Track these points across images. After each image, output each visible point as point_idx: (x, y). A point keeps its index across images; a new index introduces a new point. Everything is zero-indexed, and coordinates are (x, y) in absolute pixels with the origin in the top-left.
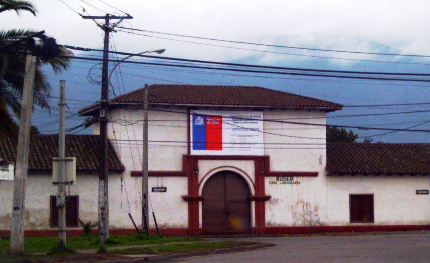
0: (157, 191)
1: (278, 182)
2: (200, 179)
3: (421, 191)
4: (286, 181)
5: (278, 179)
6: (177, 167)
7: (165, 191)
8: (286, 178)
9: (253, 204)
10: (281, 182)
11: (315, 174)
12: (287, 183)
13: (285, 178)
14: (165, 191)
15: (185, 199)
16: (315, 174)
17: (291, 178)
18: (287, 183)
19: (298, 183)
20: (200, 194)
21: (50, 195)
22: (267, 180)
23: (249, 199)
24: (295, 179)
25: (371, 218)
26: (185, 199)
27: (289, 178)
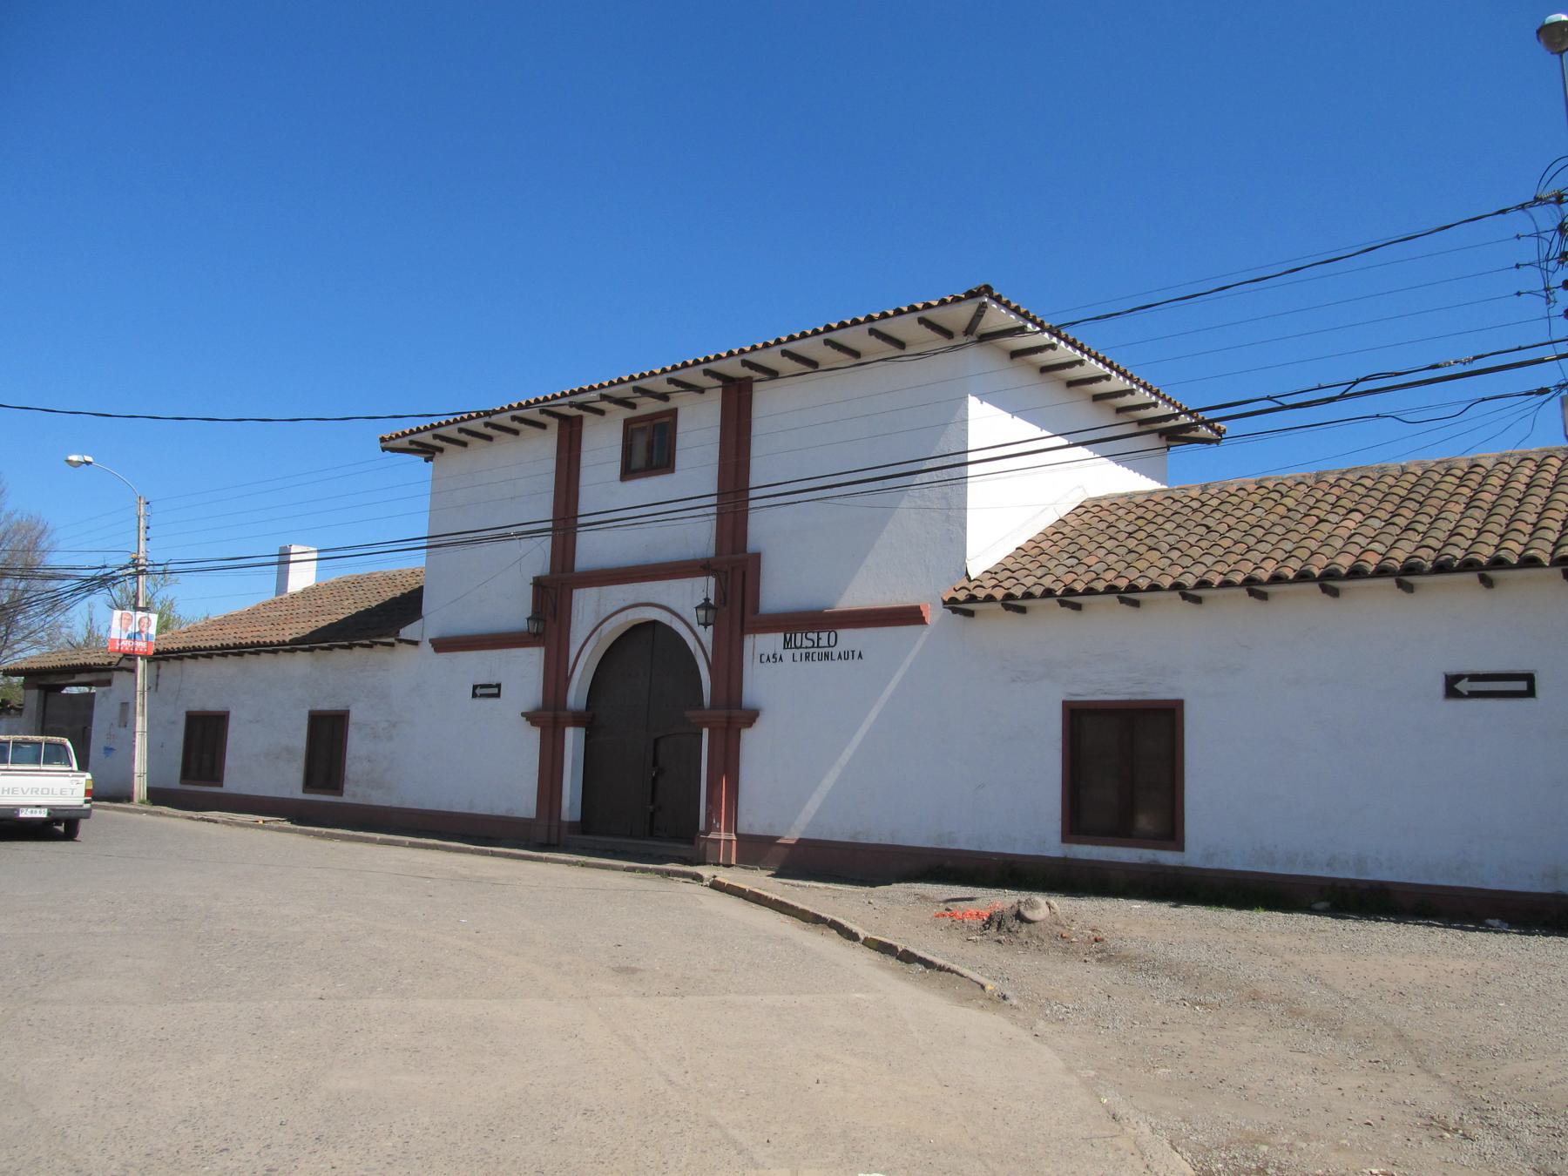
0: (482, 696)
1: (787, 654)
6: (516, 611)
7: (498, 695)
8: (813, 636)
10: (798, 652)
11: (910, 616)
13: (810, 635)
14: (1530, 693)
15: (532, 717)
17: (833, 635)
19: (856, 654)
21: (309, 708)
23: (587, 720)
24: (848, 638)
27: (824, 636)
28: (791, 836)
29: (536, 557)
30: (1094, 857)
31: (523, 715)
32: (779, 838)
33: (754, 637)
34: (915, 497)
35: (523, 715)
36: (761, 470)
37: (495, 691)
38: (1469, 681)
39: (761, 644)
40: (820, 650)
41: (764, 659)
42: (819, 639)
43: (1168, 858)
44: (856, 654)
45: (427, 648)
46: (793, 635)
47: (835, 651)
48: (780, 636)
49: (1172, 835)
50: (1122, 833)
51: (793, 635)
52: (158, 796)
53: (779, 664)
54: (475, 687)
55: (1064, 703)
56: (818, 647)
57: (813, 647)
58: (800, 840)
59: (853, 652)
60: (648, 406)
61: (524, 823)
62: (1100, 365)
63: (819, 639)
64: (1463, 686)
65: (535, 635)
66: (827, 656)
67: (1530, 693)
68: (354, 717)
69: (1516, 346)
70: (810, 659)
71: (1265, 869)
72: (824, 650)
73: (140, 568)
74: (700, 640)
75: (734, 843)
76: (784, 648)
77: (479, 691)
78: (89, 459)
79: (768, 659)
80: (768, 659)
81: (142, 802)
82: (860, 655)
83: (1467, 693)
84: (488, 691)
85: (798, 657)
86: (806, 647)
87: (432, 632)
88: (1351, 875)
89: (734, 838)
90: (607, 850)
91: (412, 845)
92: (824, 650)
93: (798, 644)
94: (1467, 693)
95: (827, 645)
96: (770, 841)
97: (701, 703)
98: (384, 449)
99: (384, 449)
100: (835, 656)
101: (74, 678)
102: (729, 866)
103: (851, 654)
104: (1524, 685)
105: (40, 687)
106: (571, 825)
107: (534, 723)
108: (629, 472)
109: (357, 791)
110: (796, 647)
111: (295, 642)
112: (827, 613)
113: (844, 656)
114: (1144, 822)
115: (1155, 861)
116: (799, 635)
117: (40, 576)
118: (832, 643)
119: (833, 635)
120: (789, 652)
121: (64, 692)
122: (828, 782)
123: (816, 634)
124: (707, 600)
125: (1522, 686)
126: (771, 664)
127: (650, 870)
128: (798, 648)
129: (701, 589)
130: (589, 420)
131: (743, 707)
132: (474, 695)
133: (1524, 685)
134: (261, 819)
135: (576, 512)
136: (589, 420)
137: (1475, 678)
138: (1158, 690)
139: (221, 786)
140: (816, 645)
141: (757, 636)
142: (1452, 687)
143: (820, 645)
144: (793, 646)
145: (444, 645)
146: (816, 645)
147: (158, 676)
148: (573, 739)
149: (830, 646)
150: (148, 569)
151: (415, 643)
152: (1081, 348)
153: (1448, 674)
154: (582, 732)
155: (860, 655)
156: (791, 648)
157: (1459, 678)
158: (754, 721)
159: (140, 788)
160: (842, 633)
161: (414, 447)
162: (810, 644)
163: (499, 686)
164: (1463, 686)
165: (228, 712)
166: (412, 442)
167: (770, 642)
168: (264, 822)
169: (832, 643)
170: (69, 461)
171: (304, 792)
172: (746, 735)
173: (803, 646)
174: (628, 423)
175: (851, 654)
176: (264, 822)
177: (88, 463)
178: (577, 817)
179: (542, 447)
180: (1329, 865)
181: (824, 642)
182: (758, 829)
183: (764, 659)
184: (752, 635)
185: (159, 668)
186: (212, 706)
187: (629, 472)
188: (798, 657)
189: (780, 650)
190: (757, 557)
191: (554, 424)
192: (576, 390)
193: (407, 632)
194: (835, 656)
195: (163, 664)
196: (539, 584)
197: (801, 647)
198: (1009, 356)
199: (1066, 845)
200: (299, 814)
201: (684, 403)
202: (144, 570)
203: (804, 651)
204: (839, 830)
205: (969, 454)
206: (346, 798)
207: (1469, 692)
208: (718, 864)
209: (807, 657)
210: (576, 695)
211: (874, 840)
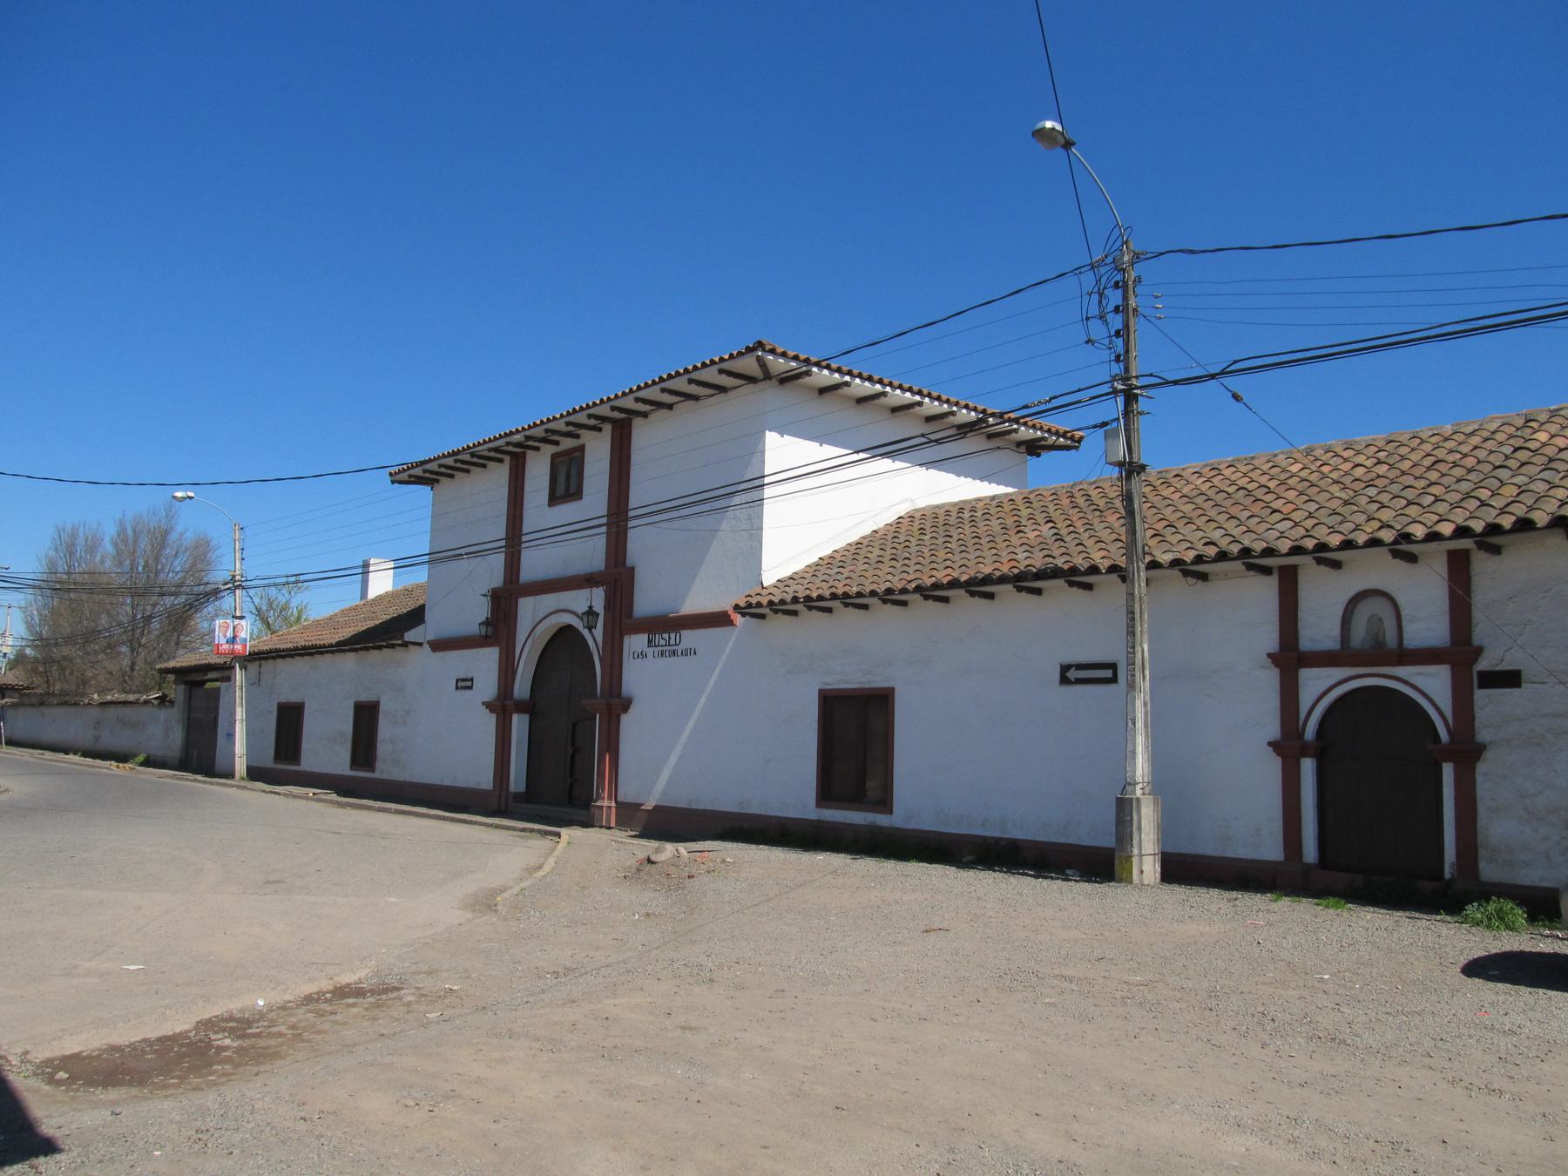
1: (650, 651)
3: (1080, 667)
7: (470, 688)
8: (666, 636)
10: (656, 649)
15: (489, 706)
21: (354, 699)
24: (689, 637)
26: (489, 706)
27: (673, 635)
28: (649, 805)
29: (491, 571)
31: (483, 703)
32: (642, 805)
35: (483, 703)
36: (639, 495)
37: (469, 684)
41: (636, 656)
42: (670, 638)
43: (881, 820)
45: (427, 647)
47: (679, 649)
49: (884, 803)
50: (856, 799)
52: (255, 774)
53: (645, 659)
54: (457, 681)
55: (821, 691)
56: (669, 645)
60: (567, 443)
62: (908, 395)
63: (670, 638)
65: (486, 637)
66: (674, 653)
68: (382, 708)
69: (1077, 389)
71: (943, 829)
73: (236, 584)
74: (595, 638)
75: (613, 810)
77: (460, 684)
78: (191, 494)
81: (243, 779)
82: (695, 653)
84: (465, 684)
86: (662, 646)
87: (430, 637)
88: (996, 834)
89: (613, 804)
96: (636, 807)
97: (596, 694)
98: (393, 482)
99: (393, 482)
100: (680, 653)
101: (206, 675)
102: (609, 828)
105: (185, 683)
106: (517, 796)
107: (491, 711)
108: (554, 499)
109: (386, 769)
110: (655, 646)
111: (339, 644)
112: (673, 617)
113: (686, 653)
116: (657, 636)
120: (651, 649)
121: (206, 687)
122: (673, 759)
124: (591, 607)
126: (639, 660)
127: (514, 829)
129: (596, 598)
130: (530, 453)
131: (623, 695)
132: (457, 688)
134: (310, 791)
136: (530, 453)
138: (880, 682)
139: (299, 764)
141: (632, 636)
145: (439, 645)
147: (260, 673)
148: (519, 723)
149: (676, 645)
150: (244, 584)
151: (420, 644)
152: (880, 382)
154: (526, 718)
158: (629, 708)
159: (240, 767)
160: (685, 633)
161: (412, 479)
163: (472, 680)
165: (304, 703)
166: (410, 476)
168: (314, 794)
170: (174, 497)
171: (351, 769)
172: (625, 719)
174: (554, 457)
176: (314, 794)
177: (191, 498)
178: (522, 788)
179: (498, 476)
181: (672, 642)
185: (260, 666)
186: (293, 698)
187: (554, 499)
188: (656, 653)
190: (633, 569)
191: (507, 458)
192: (508, 432)
193: (410, 636)
194: (680, 653)
195: (263, 662)
197: (658, 645)
198: (817, 393)
199: (820, 810)
200: (346, 788)
201: (587, 437)
202: (240, 585)
204: (682, 798)
205: (766, 478)
206: (377, 775)
207: (1075, 679)
208: (601, 827)
209: (662, 654)
210: (522, 687)
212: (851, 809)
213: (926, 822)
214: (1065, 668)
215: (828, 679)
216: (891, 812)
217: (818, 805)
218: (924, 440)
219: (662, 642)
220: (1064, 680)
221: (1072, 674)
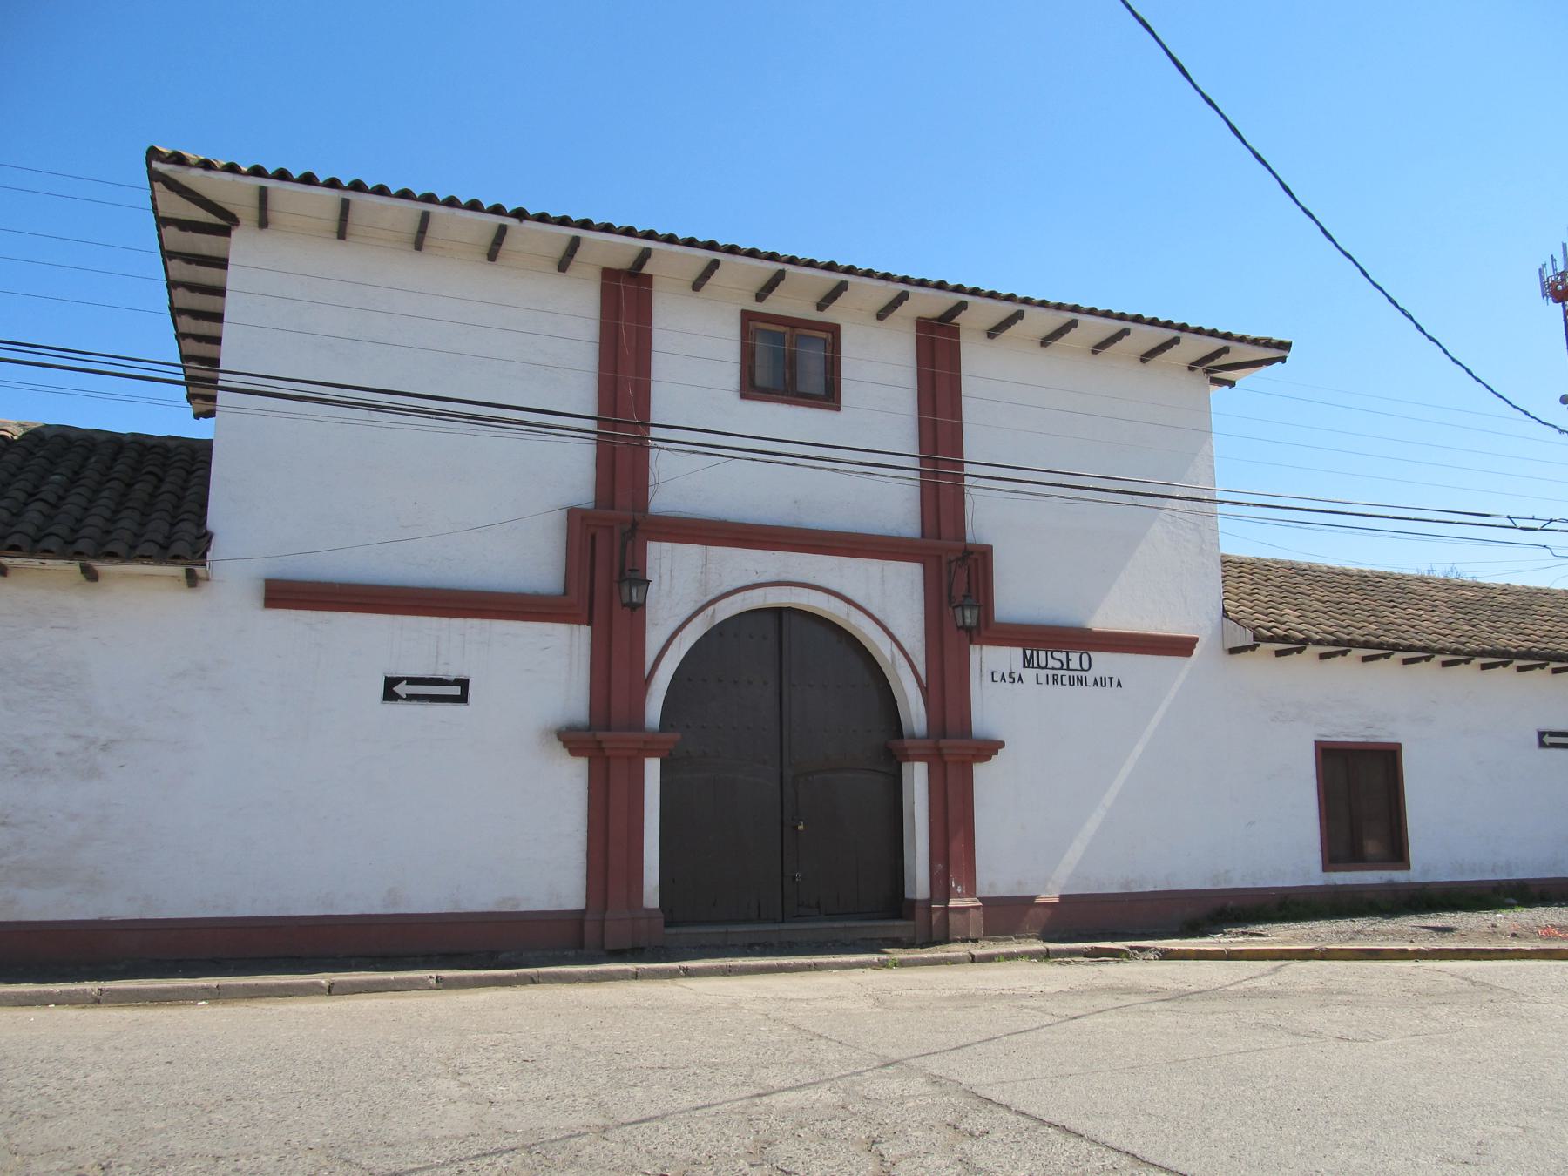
0: (411, 698)
1: (1029, 674)
2: (654, 640)
4: (1060, 673)
5: (1027, 662)
8: (1063, 656)
9: (917, 777)
10: (1042, 673)
11: (1181, 647)
12: (1066, 680)
13: (1056, 654)
14: (463, 699)
15: (571, 739)
16: (1181, 647)
17: (1085, 657)
18: (1066, 680)
19: (1115, 682)
20: (653, 711)
22: (988, 660)
24: (1103, 662)
25: (1397, 854)
26: (571, 739)
27: (1074, 657)
28: (1050, 895)
30: (1348, 882)
32: (1034, 897)
33: (981, 649)
34: (1168, 522)
36: (978, 442)
37: (456, 691)
38: (407, 684)
39: (988, 660)
40: (1071, 673)
41: (997, 677)
42: (1068, 660)
43: (1399, 876)
44: (1115, 682)
46: (1035, 652)
47: (1090, 676)
48: (1019, 651)
51: (1035, 652)
56: (1068, 669)
57: (1061, 668)
58: (1062, 897)
59: (1111, 678)
61: (577, 918)
63: (1068, 660)
64: (402, 689)
66: (1080, 681)
67: (463, 699)
70: (1059, 681)
72: (1076, 674)
76: (1024, 666)
79: (1003, 678)
80: (1003, 678)
82: (1119, 683)
83: (405, 696)
85: (1042, 679)
86: (1053, 669)
88: (1504, 877)
90: (751, 946)
91: (332, 990)
92: (1076, 674)
93: (1043, 664)
94: (405, 696)
95: (1079, 668)
96: (1025, 903)
100: (1090, 681)
103: (1108, 680)
104: (460, 691)
110: (1039, 667)
113: (1101, 682)
114: (1372, 847)
115: (1390, 881)
116: (1042, 654)
117: (832, 380)
118: (1085, 666)
119: (1085, 657)
122: (1091, 827)
123: (1065, 653)
125: (456, 691)
126: (1007, 685)
128: (1043, 668)
133: (460, 691)
135: (648, 417)
137: (412, 681)
138: (1383, 736)
140: (1065, 667)
141: (985, 647)
142: (390, 690)
143: (1071, 667)
144: (1036, 665)
146: (1065, 667)
149: (1083, 670)
153: (388, 676)
155: (1119, 683)
156: (1033, 667)
157: (398, 680)
162: (1058, 665)
164: (402, 689)
167: (1007, 657)
169: (1085, 666)
172: (980, 771)
173: (1049, 666)
175: (1108, 680)
180: (1493, 871)
181: (1074, 664)
182: (1003, 890)
183: (997, 677)
184: (977, 647)
188: (1042, 679)
189: (1018, 667)
194: (1090, 681)
196: (576, 517)
197: (1046, 668)
199: (1326, 873)
203: (1051, 673)
204: (1109, 878)
211: (1149, 888)
212: (1396, 869)
213: (1442, 874)
214: (1541, 734)
215: (1323, 731)
216: (1408, 867)
217: (1325, 869)
218: (1509, 523)
219: (1052, 663)
220: (1542, 744)
221: (1547, 740)
